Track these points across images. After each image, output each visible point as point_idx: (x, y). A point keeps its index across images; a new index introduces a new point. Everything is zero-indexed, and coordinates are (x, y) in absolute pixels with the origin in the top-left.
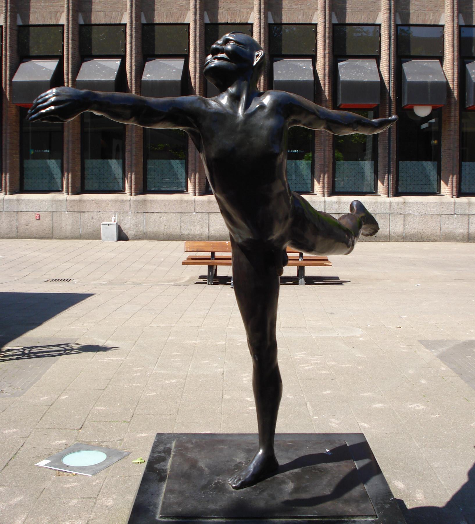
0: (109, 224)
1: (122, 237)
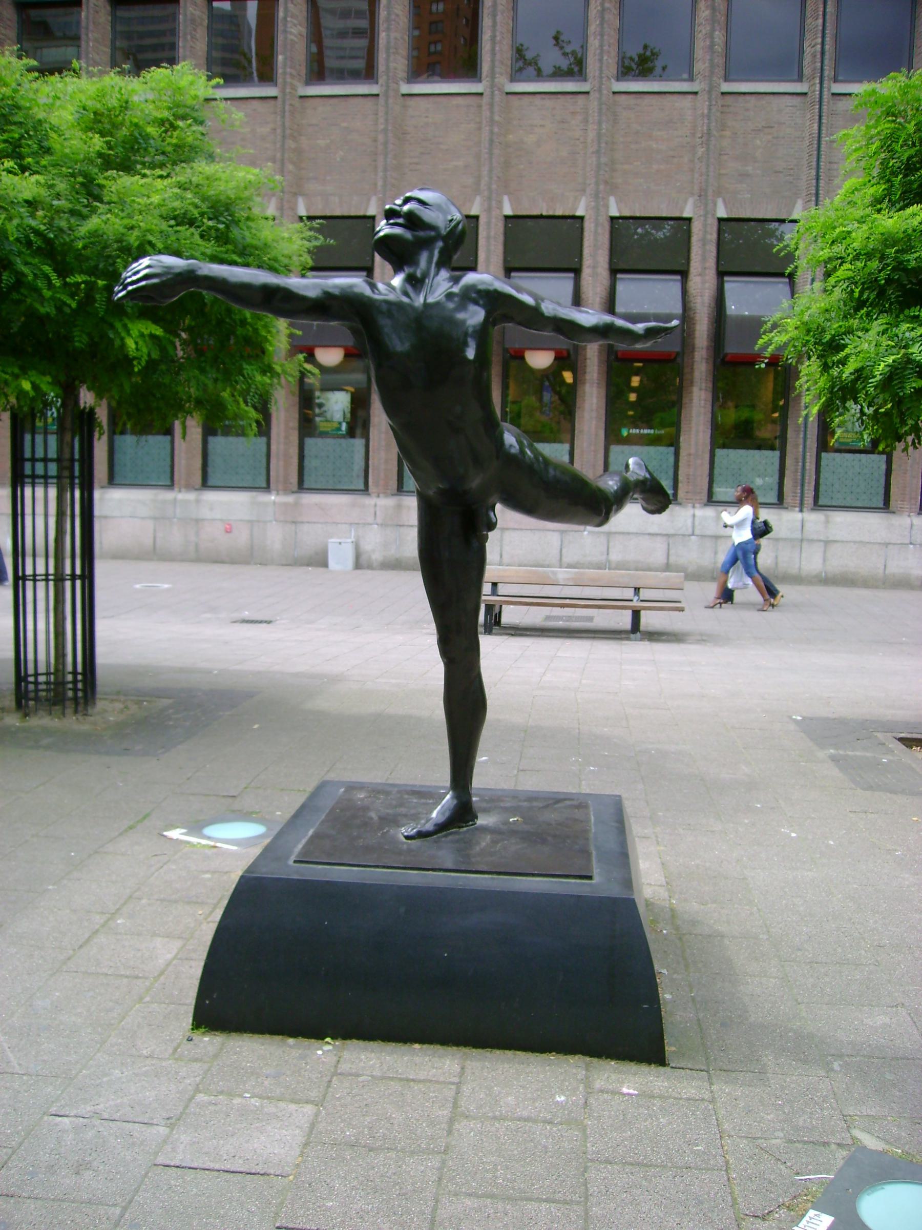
0: (340, 543)
1: (359, 564)
